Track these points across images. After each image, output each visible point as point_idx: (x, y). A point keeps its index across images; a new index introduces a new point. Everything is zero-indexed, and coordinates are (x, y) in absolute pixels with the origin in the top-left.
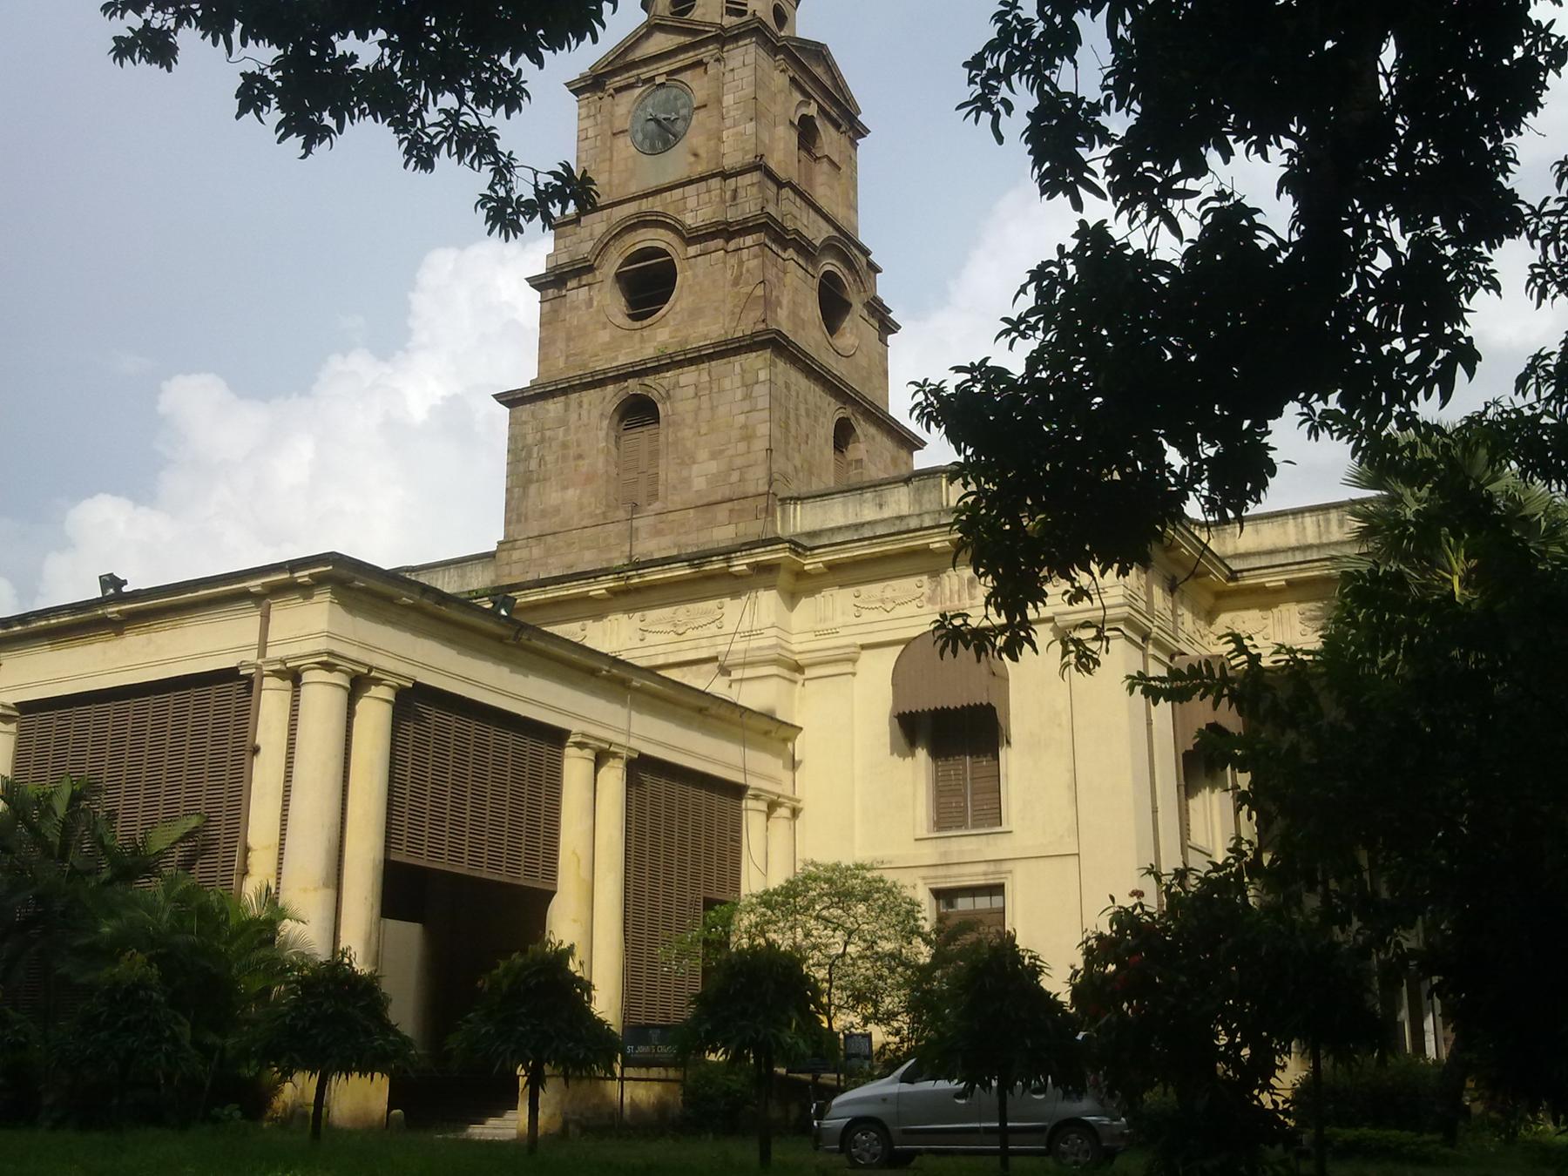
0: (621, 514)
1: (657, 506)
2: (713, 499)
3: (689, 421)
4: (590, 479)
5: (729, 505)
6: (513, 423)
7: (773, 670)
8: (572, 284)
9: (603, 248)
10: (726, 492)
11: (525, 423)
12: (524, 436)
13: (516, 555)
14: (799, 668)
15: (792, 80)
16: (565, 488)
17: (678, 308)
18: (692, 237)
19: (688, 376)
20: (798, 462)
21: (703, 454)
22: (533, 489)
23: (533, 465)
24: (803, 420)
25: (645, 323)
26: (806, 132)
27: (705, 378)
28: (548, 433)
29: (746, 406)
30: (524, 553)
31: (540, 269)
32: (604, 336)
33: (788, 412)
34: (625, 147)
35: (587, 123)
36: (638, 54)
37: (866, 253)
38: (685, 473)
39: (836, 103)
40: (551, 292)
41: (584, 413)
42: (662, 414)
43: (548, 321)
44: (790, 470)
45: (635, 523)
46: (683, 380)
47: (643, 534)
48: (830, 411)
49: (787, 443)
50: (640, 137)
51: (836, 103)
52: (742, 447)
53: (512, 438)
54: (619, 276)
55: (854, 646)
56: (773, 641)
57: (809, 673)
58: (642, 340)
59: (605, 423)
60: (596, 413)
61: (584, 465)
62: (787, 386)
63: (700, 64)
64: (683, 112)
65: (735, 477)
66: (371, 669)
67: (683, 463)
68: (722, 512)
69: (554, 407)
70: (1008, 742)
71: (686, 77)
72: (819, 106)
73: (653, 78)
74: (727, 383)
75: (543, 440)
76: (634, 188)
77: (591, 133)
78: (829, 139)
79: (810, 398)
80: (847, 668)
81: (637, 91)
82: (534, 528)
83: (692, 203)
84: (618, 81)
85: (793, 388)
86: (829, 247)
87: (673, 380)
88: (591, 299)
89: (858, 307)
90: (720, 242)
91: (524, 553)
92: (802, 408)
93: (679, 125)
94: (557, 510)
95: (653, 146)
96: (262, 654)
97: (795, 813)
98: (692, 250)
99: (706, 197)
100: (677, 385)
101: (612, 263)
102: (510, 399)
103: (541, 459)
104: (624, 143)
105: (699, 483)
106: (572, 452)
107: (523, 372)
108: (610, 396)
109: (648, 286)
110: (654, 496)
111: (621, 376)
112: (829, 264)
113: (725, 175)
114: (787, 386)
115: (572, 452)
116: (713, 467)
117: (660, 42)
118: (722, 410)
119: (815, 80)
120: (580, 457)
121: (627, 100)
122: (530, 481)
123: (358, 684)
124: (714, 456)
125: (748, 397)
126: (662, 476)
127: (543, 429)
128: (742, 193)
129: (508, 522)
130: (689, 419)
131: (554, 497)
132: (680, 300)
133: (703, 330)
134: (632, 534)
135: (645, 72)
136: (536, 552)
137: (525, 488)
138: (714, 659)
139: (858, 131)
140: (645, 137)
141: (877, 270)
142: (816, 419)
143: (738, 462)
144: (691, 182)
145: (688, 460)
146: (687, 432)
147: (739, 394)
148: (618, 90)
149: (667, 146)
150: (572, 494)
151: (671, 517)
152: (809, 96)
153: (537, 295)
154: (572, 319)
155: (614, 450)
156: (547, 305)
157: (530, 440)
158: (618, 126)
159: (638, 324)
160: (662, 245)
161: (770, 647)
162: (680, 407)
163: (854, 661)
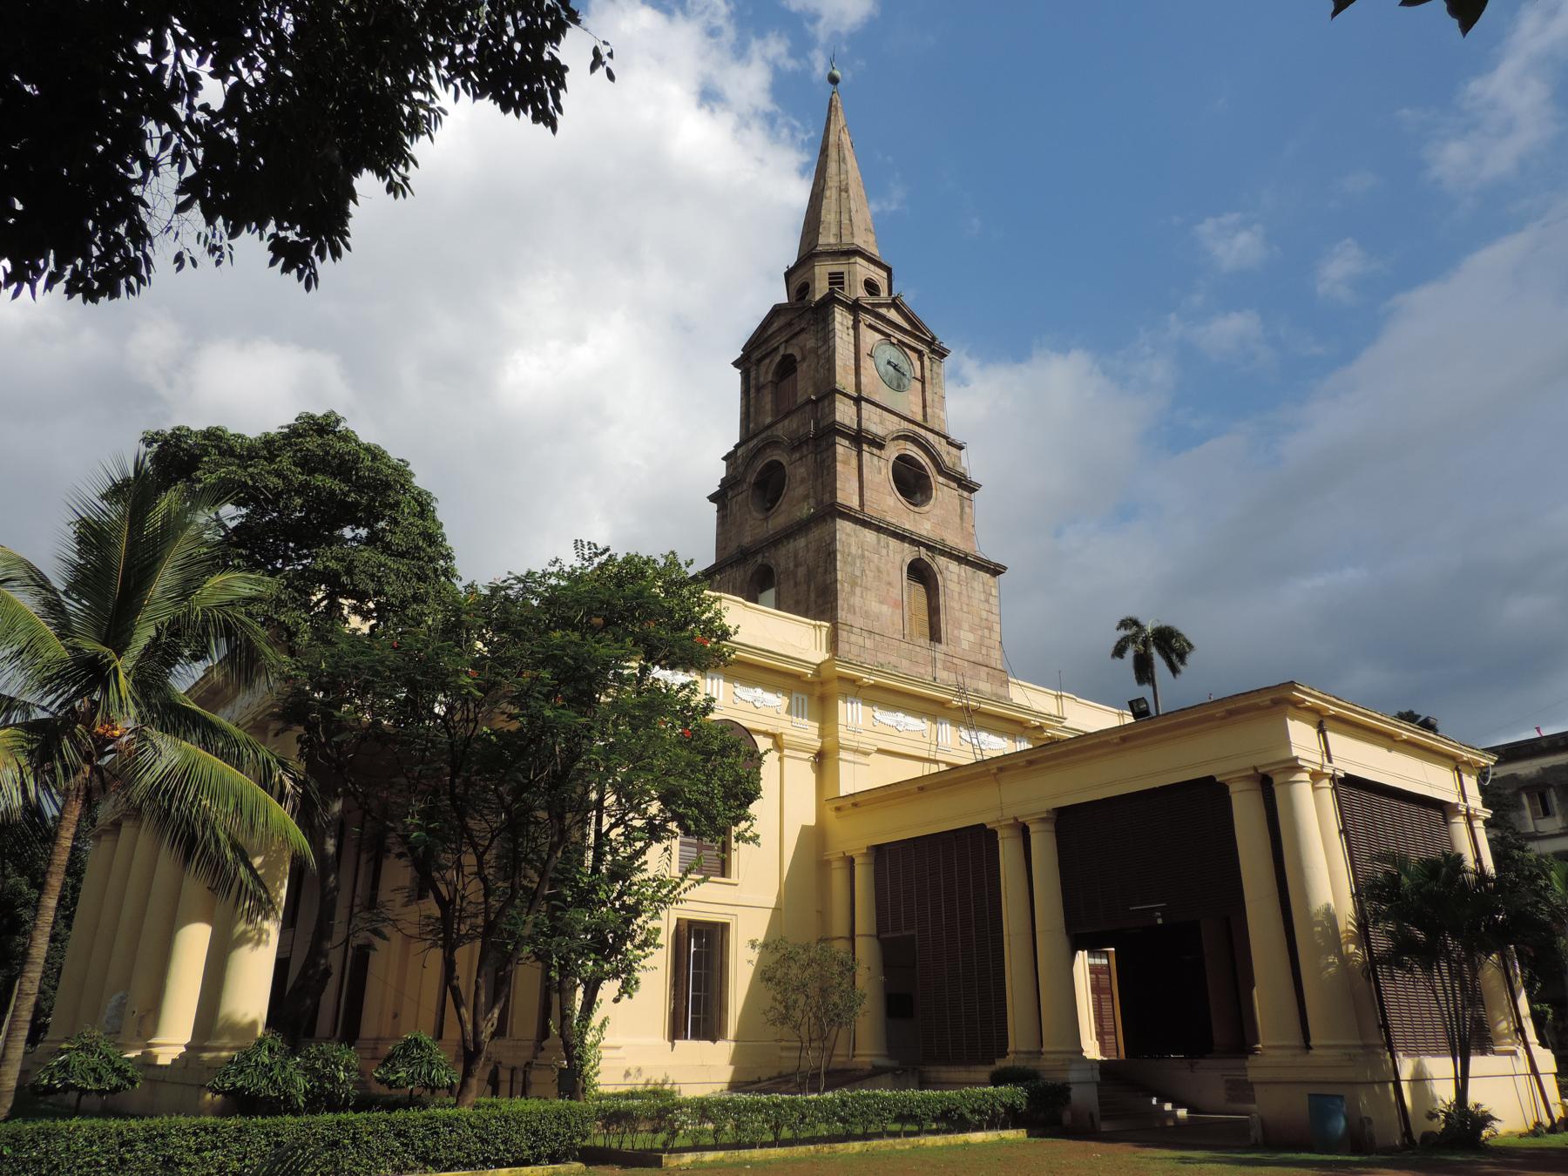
12: (849, 545)
13: (853, 638)
16: (881, 602)
19: (954, 566)
21: (966, 626)
22: (858, 590)
30: (860, 641)
60: (898, 558)
81: (878, 336)
84: (869, 319)
91: (860, 641)
98: (941, 479)
101: (892, 451)
108: (908, 553)
124: (972, 630)
130: (956, 596)
131: (874, 606)
136: (868, 643)
143: (987, 642)
150: (885, 608)
157: (853, 551)
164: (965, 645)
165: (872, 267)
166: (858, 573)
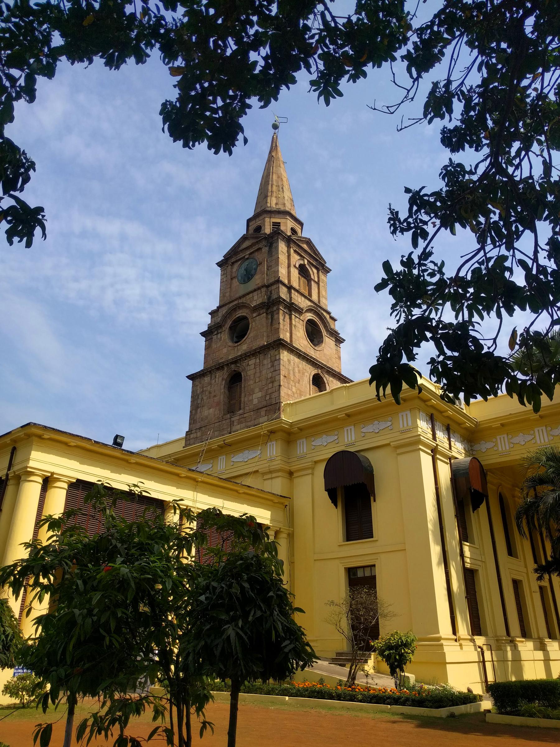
0: (228, 416)
1: (241, 412)
2: (260, 406)
3: (252, 378)
4: (218, 404)
5: (265, 409)
6: (194, 386)
7: (280, 474)
8: (216, 333)
9: (225, 318)
10: (264, 403)
11: (197, 386)
13: (192, 436)
14: (291, 473)
15: (295, 251)
17: (250, 336)
18: (255, 309)
19: (252, 362)
20: (294, 390)
21: (257, 390)
22: (199, 410)
23: (199, 401)
24: (297, 375)
25: (239, 343)
26: (303, 270)
27: (258, 361)
28: (205, 389)
29: (272, 369)
31: (205, 328)
32: (225, 350)
33: (289, 370)
34: (235, 282)
35: (223, 277)
36: (241, 248)
37: (329, 313)
38: (250, 398)
39: (316, 260)
40: (208, 338)
41: (217, 379)
42: (243, 376)
43: (207, 348)
44: (290, 392)
45: (232, 419)
46: (250, 363)
47: (235, 424)
48: (312, 371)
49: (289, 383)
50: (240, 278)
51: (316, 260)
52: (270, 385)
53: (193, 392)
54: (230, 328)
55: (312, 461)
56: (279, 462)
57: (295, 475)
58: (238, 350)
59: (224, 382)
60: (221, 379)
61: (216, 399)
62: (289, 361)
63: (259, 249)
64: (254, 267)
65: (268, 398)
66: (53, 474)
67: (250, 395)
68: (263, 412)
69: (207, 379)
70: (375, 501)
71: (256, 254)
72: (308, 260)
73: (244, 257)
74: (265, 362)
75: (203, 391)
76: (237, 296)
77: (225, 280)
78: (313, 272)
79: (300, 366)
80: (310, 471)
81: (239, 263)
82: (198, 425)
83: (256, 298)
84: (233, 260)
85: (292, 362)
86: (309, 310)
87: (247, 363)
88: (221, 338)
89: (324, 333)
90: (264, 310)
92: (296, 369)
93: (253, 272)
94: (207, 417)
95: (244, 281)
96: (9, 469)
97: (291, 536)
98: (255, 315)
99: (260, 295)
100: (248, 365)
101: (229, 323)
102: (191, 377)
103: (202, 398)
104: (235, 282)
105: (255, 401)
106: (212, 395)
107: (198, 366)
109: (239, 330)
110: (240, 409)
111: (228, 364)
112: (309, 316)
113: (268, 286)
114: (289, 361)
115: (212, 395)
116: (259, 395)
117: (247, 244)
118: (264, 372)
119: (305, 251)
120: (215, 396)
121: (236, 266)
122: (198, 407)
123: (48, 482)
124: (260, 391)
125: (273, 366)
126: (242, 399)
127: (203, 387)
128: (273, 292)
129: (190, 424)
130: (252, 378)
132: (251, 334)
133: (258, 343)
134: (232, 424)
135: (241, 255)
136: (199, 434)
137: (196, 410)
138: (257, 471)
139: (327, 271)
140: (242, 278)
141: (335, 320)
142: (303, 374)
143: (270, 391)
144: (255, 290)
145: (252, 392)
146: (251, 382)
147: (269, 366)
148: (233, 263)
149: (249, 279)
150: (212, 410)
151: (245, 415)
152: (304, 258)
153: (204, 339)
154: (214, 346)
155: (227, 392)
156: (207, 342)
158: (234, 275)
159: (236, 345)
160: (245, 314)
161: (279, 464)
162: (249, 373)
163: (313, 469)
164: (255, 401)
165: (257, 220)
166: (199, 401)
